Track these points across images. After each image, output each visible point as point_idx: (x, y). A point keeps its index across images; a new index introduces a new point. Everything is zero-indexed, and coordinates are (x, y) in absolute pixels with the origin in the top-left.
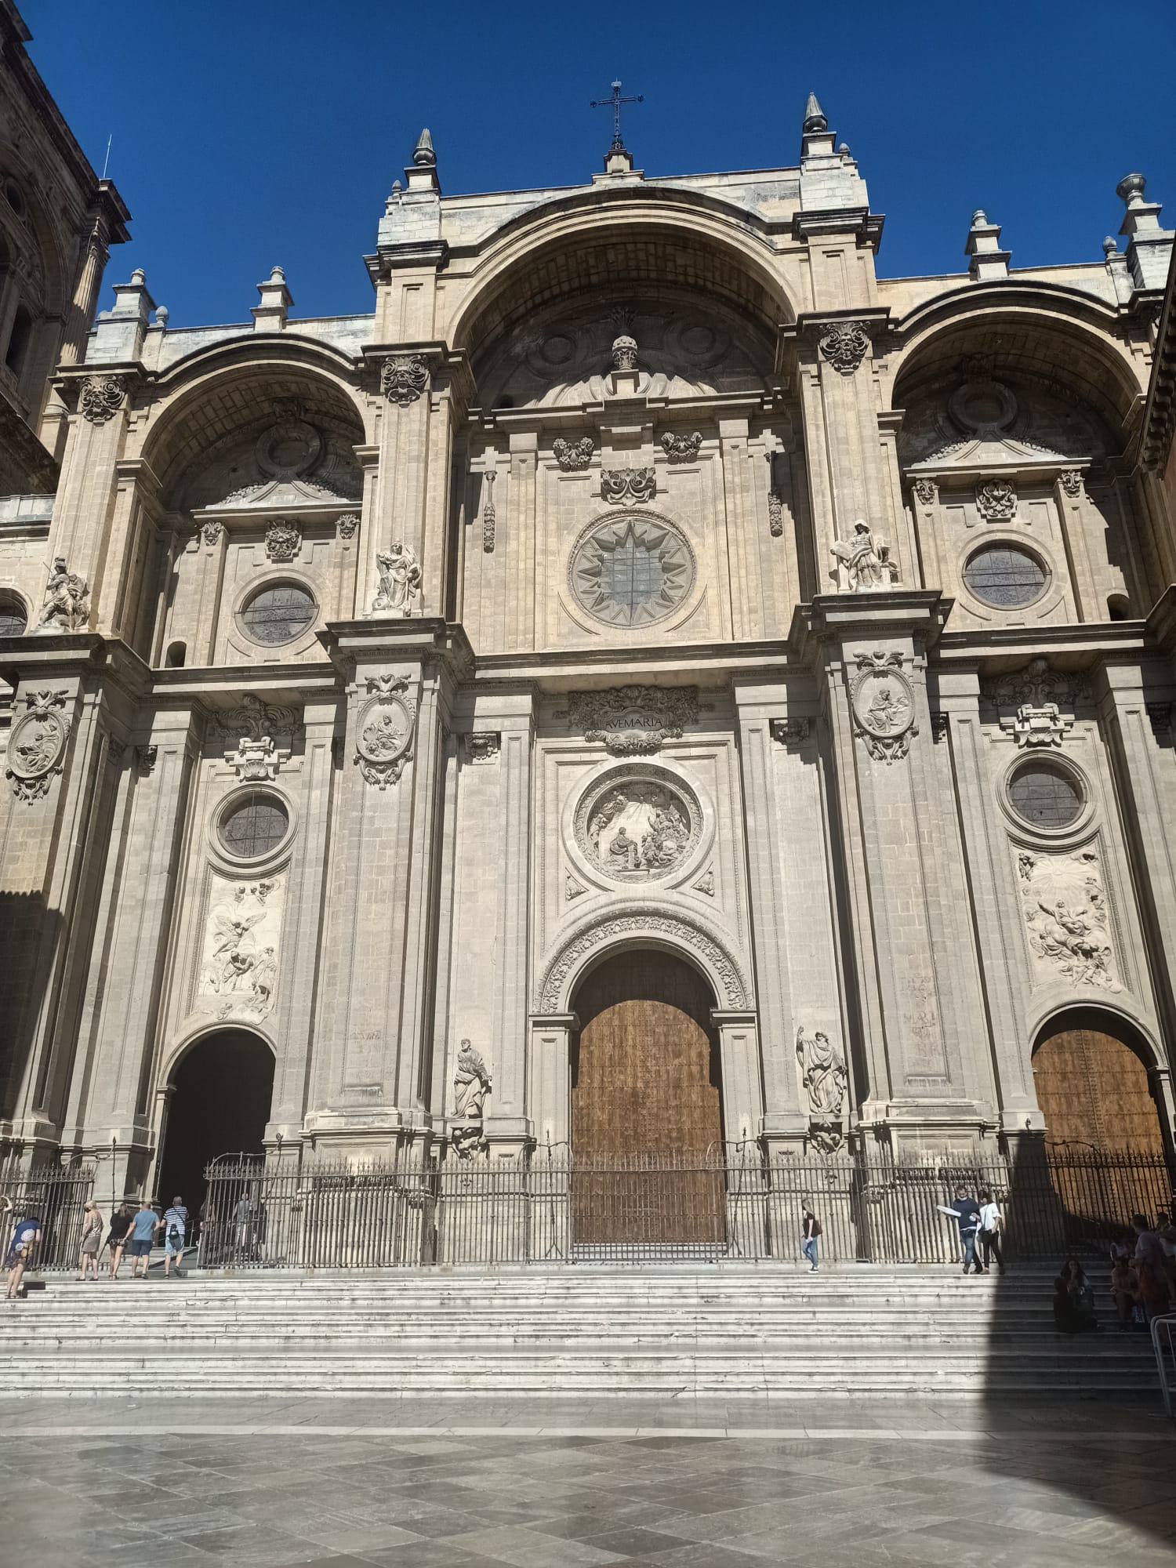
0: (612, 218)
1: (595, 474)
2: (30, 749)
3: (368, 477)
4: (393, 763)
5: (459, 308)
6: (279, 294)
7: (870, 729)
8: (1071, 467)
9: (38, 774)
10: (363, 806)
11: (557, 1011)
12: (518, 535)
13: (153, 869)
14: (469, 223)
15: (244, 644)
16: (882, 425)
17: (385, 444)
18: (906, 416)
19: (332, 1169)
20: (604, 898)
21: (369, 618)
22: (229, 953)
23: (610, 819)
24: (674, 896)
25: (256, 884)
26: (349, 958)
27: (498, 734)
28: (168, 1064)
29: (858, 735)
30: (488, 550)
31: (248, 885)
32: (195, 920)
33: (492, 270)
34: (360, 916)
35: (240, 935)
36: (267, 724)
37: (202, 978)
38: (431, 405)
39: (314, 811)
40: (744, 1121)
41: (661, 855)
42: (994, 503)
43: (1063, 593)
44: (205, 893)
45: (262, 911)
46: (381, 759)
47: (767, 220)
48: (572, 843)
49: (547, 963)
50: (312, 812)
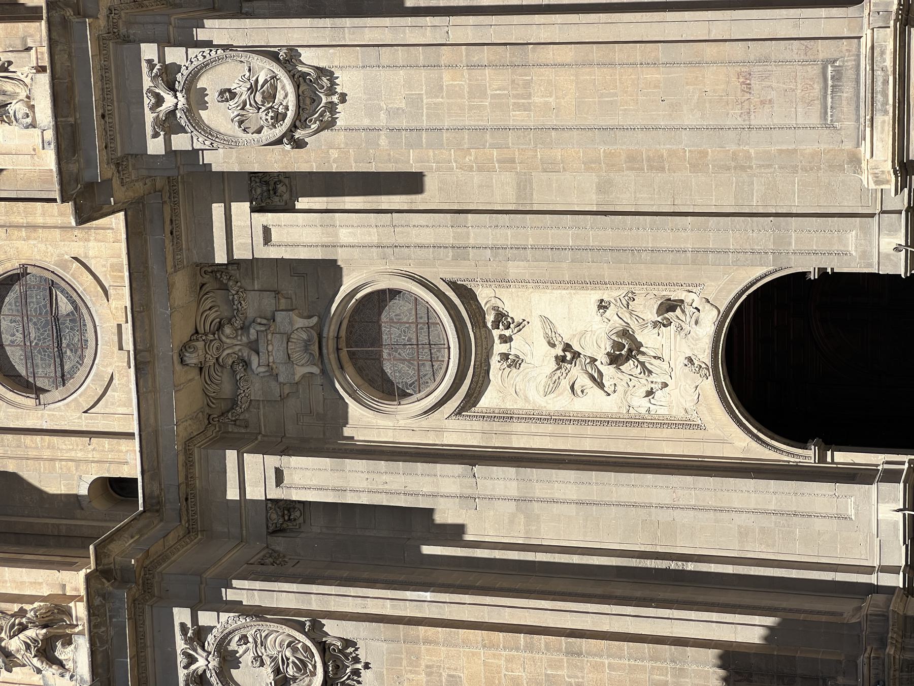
2: (277, 671)
9: (317, 658)
13: (468, 492)
15: (92, 387)
21: (50, 135)
22: (601, 368)
26: (619, 133)
28: (776, 449)
32: (549, 428)
34: (553, 121)
35: (577, 355)
36: (228, 330)
37: (643, 411)
39: (372, 236)
44: (507, 416)
50: (375, 239)
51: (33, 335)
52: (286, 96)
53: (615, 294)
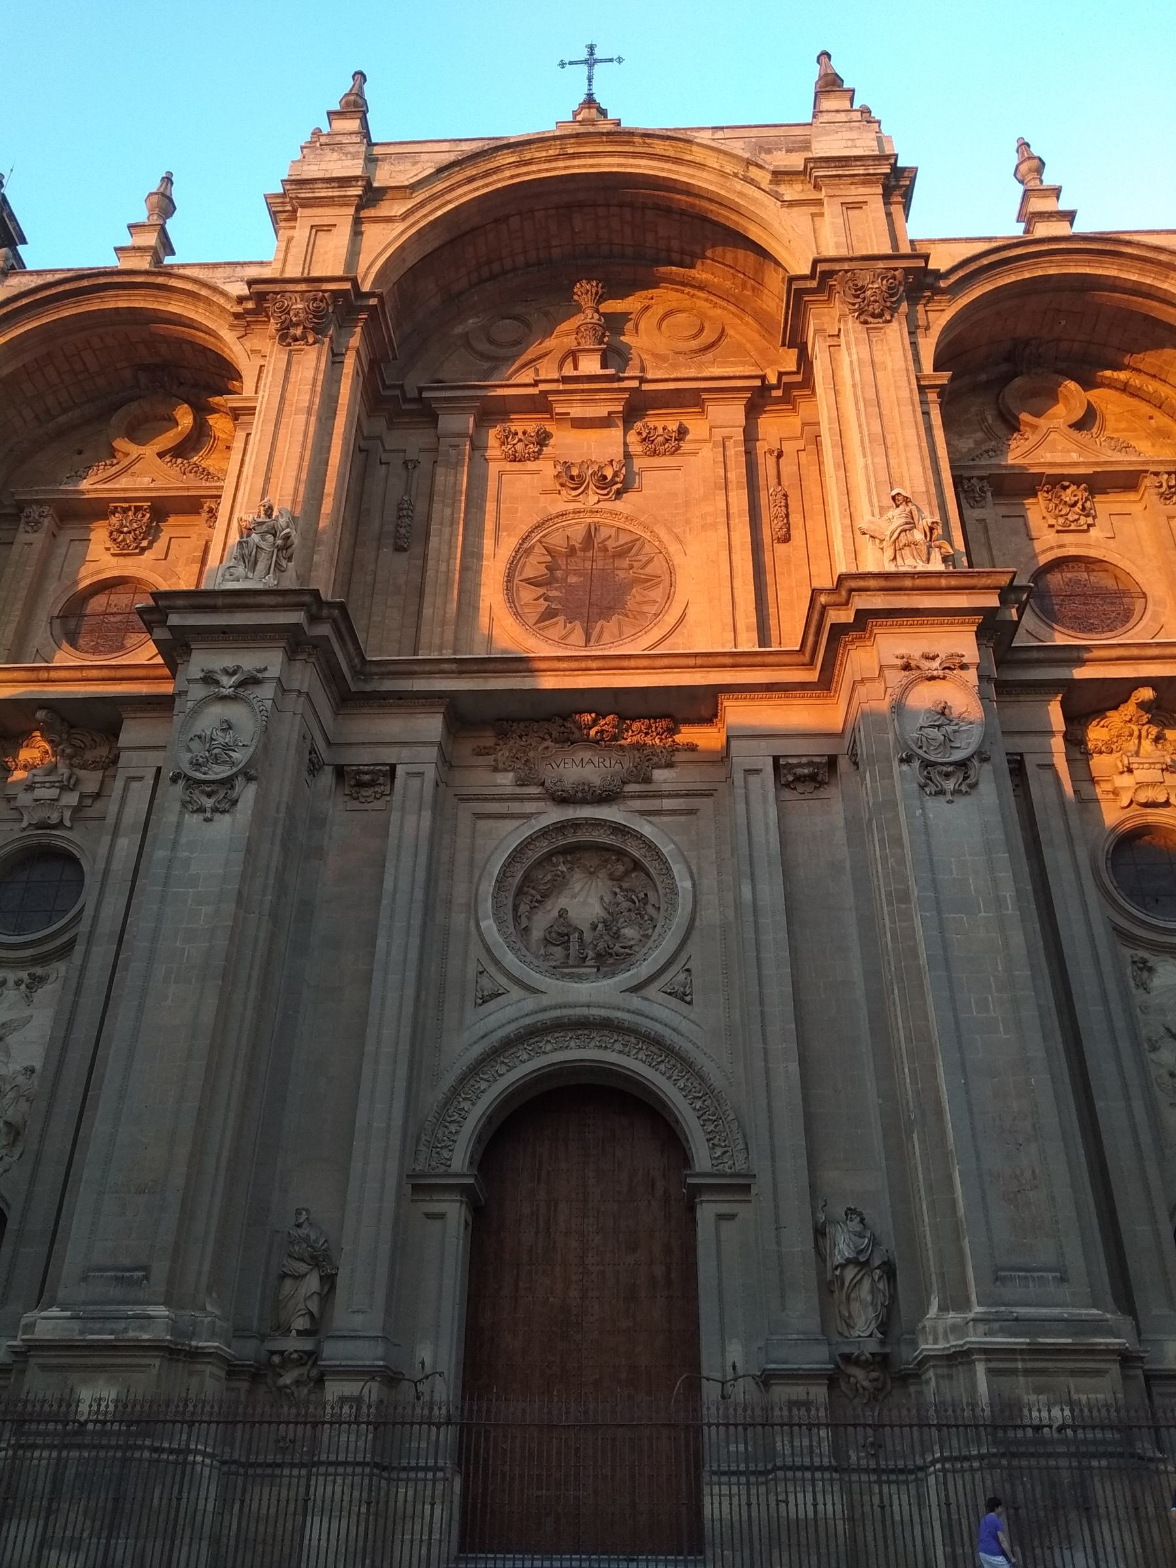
0: (579, 166)
1: (547, 469)
3: (241, 435)
4: (228, 782)
5: (380, 254)
6: (156, 234)
7: (920, 752)
8: (1161, 469)
10: (175, 845)
11: (451, 1170)
12: (441, 530)
14: (401, 168)
16: (922, 389)
17: (267, 391)
18: (952, 379)
19: (46, 1408)
20: (530, 1003)
23: (545, 896)
24: (635, 1002)
25: (23, 975)
27: (393, 767)
29: (902, 761)
30: (399, 549)
31: (11, 976)
33: (425, 216)
38: (334, 355)
39: (116, 865)
40: (735, 1352)
41: (617, 948)
42: (1065, 510)
43: (1163, 620)
45: (27, 1013)
46: (211, 777)
47: (771, 168)
48: (488, 924)
49: (441, 1097)
51: (112, 619)
52: (216, 774)
53: (36, 1084)
